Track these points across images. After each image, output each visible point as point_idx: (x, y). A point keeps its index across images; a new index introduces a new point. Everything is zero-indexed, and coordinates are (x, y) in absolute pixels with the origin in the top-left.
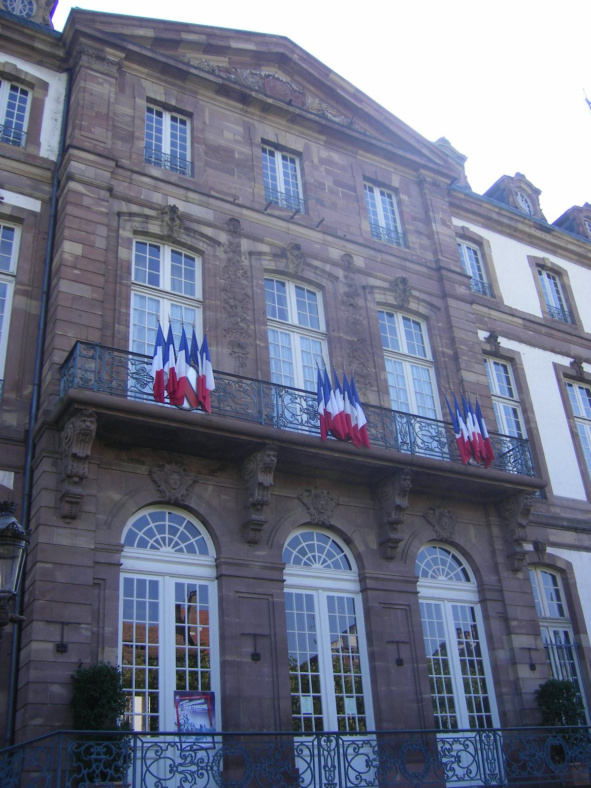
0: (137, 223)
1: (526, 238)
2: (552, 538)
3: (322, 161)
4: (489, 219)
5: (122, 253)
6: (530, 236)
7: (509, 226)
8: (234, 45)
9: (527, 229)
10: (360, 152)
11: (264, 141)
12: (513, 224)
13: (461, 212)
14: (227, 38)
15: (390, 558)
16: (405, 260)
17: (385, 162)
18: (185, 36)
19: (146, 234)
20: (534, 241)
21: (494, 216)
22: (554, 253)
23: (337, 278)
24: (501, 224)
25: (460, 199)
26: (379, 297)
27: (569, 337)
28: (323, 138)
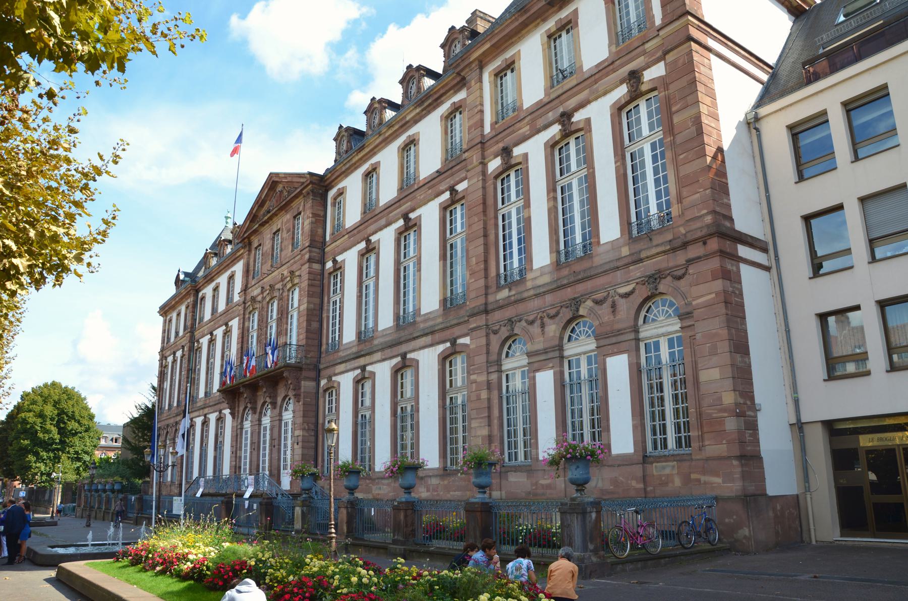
4: (344, 172)
6: (361, 159)
9: (357, 158)
22: (375, 154)
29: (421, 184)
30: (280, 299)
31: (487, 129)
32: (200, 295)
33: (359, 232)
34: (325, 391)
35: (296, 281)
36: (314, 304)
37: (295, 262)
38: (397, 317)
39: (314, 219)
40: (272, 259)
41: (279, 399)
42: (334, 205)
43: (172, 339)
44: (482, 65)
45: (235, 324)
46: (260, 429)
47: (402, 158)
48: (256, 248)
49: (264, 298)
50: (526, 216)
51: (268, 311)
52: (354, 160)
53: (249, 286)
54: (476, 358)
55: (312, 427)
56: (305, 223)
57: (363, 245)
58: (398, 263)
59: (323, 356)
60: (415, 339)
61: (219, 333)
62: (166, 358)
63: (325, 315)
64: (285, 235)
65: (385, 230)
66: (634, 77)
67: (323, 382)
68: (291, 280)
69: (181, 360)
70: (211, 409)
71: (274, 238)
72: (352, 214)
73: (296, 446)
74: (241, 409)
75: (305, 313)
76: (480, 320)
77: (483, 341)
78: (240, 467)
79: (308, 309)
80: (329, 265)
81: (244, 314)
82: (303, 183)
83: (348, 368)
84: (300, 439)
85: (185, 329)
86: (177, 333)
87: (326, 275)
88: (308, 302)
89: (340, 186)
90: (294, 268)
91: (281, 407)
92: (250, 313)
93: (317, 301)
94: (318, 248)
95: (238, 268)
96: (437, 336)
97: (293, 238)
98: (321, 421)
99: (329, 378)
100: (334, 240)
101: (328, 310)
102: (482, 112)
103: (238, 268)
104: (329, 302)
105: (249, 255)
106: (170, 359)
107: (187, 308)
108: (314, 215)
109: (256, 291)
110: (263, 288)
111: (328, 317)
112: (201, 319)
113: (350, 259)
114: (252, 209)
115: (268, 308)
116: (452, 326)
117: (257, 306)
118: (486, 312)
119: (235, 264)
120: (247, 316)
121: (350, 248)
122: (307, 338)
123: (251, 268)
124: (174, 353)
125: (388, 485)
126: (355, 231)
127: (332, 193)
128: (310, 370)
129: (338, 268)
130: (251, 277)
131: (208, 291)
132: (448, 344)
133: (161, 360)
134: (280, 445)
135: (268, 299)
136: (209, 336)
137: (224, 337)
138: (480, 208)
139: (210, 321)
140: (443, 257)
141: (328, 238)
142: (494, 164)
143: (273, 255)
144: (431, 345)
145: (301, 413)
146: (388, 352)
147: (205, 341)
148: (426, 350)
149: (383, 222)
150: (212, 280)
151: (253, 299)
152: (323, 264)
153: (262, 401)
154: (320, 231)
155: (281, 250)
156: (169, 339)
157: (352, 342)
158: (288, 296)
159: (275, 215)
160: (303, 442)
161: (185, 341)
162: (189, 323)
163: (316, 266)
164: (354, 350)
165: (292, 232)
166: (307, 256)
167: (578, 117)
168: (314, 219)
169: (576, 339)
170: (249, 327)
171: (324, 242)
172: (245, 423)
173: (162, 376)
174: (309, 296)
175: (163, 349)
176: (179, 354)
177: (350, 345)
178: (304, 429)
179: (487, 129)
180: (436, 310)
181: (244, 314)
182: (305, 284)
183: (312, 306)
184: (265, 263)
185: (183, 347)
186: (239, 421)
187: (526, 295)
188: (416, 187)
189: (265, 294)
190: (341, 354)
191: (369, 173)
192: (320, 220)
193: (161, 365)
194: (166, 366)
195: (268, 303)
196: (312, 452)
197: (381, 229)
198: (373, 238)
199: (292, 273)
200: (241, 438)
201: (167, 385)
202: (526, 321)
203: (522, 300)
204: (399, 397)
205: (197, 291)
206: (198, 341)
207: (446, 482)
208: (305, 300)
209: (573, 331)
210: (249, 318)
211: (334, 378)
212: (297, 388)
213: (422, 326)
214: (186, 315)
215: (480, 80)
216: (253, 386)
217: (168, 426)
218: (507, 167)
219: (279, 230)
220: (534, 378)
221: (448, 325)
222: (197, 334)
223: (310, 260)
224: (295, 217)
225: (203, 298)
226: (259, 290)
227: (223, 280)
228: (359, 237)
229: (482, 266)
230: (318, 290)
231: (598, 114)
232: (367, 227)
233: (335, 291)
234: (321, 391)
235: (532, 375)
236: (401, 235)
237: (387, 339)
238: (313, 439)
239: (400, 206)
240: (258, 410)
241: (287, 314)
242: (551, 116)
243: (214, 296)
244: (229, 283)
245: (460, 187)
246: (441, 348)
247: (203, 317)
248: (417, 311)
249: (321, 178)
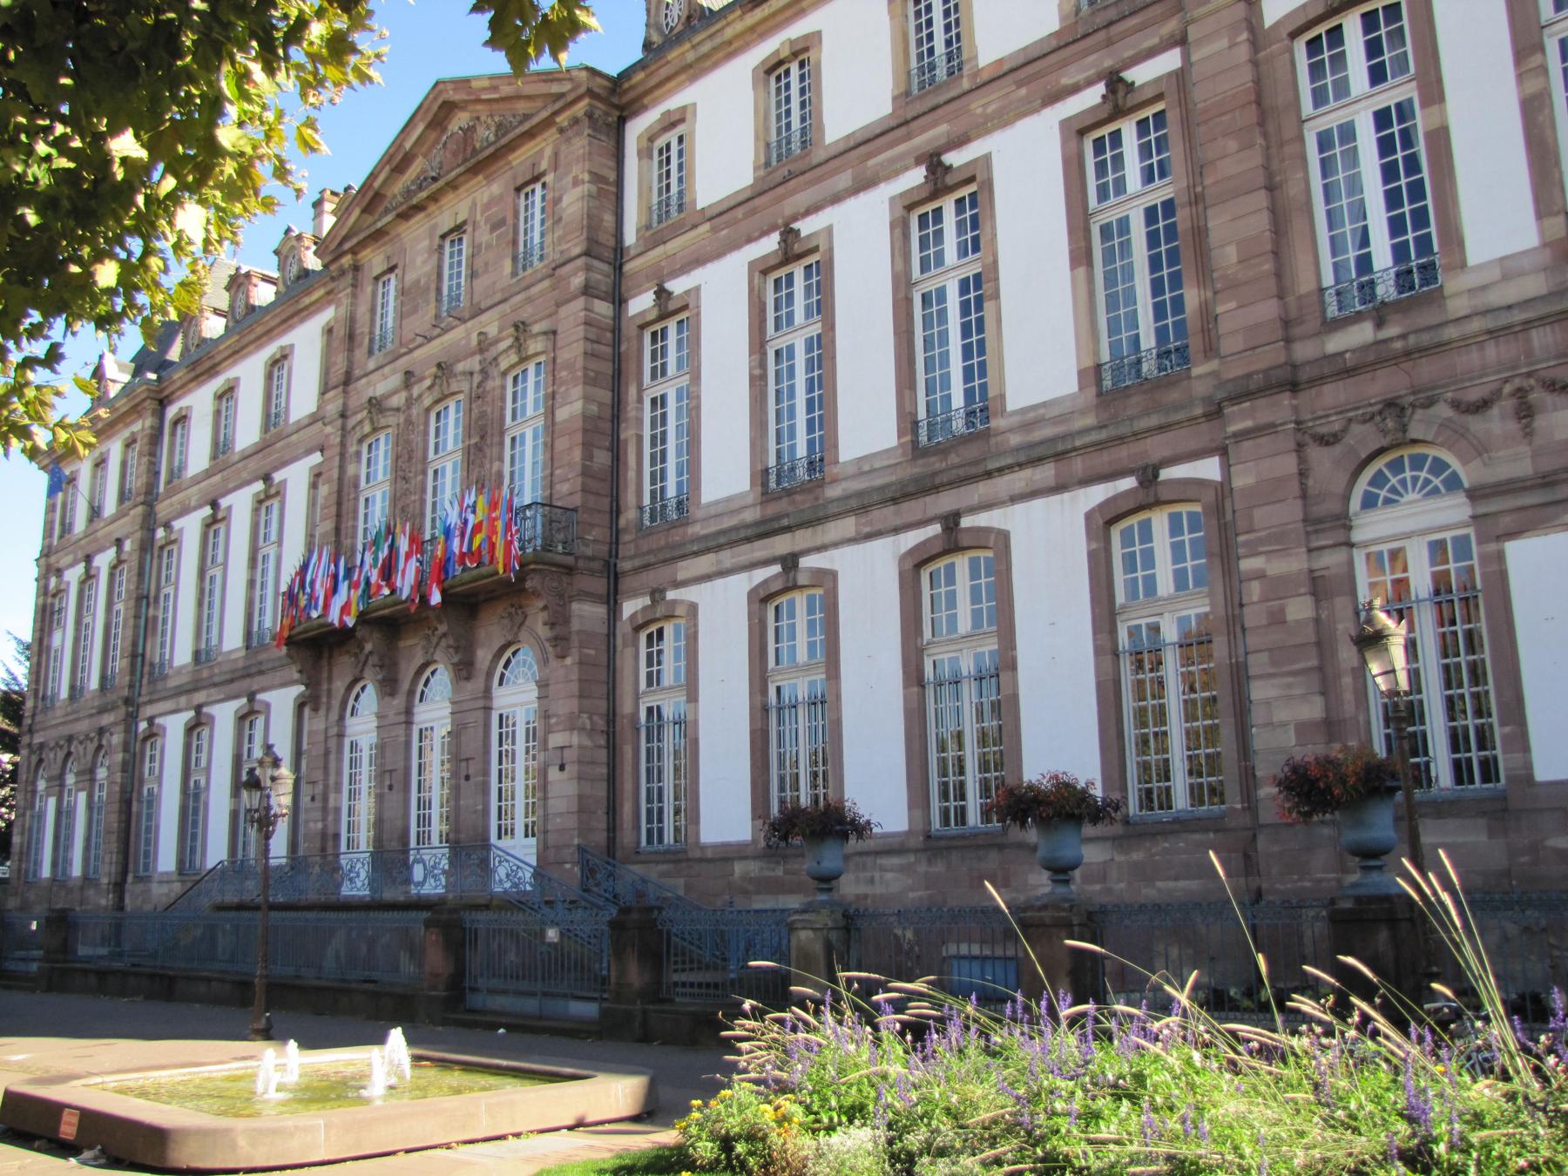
0: (358, 435)
1: (748, 38)
2: (681, 576)
3: (487, 207)
4: (690, 66)
5: (351, 470)
6: (752, 29)
7: (715, 49)
8: (408, 145)
9: (739, 27)
10: (510, 158)
11: (443, 237)
12: (718, 40)
13: (657, 93)
14: (401, 146)
15: (468, 679)
16: (528, 288)
17: (532, 143)
18: (377, 184)
19: (366, 436)
20: (759, 30)
21: (691, 57)
23: (471, 374)
24: (706, 56)
25: (643, 81)
26: (504, 365)
27: (781, 190)
28: (480, 177)
29: (985, 77)
32: (172, 412)
33: (753, 212)
34: (638, 629)
35: (534, 346)
36: (600, 404)
37: (529, 300)
38: (908, 423)
39: (594, 189)
40: (439, 300)
41: (483, 656)
43: (80, 524)
45: (296, 477)
46: (409, 736)
48: (377, 278)
49: (410, 402)
50: (1435, 123)
51: (426, 433)
52: (729, 33)
53: (357, 372)
54: (1258, 513)
55: (601, 723)
57: (770, 244)
59: (626, 538)
60: (989, 475)
61: (240, 503)
62: (59, 572)
63: (627, 433)
64: (484, 236)
65: (851, 204)
67: (631, 607)
68: (518, 345)
69: (112, 576)
70: (215, 693)
71: (441, 247)
73: (554, 774)
74: (339, 686)
75: (579, 424)
76: (1281, 408)
77: (1289, 464)
78: (337, 836)
79: (586, 417)
80: (641, 303)
81: (343, 445)
82: (561, 96)
83: (728, 564)
84: (569, 755)
85: (123, 496)
86: (95, 512)
87: (629, 330)
88: (587, 398)
89: (673, 103)
90: (525, 314)
91: (489, 675)
92: (360, 441)
93: (605, 396)
94: (608, 260)
95: (306, 342)
96: (1078, 465)
97: (515, 242)
98: (626, 707)
99: (657, 594)
100: (653, 237)
101: (640, 421)
103: (306, 342)
104: (640, 400)
105: (354, 296)
106: (74, 575)
107: (129, 445)
108: (597, 178)
109: (384, 384)
110: (408, 374)
111: (640, 438)
112: (174, 474)
113: (721, 290)
114: (373, 176)
115: (427, 424)
116: (1137, 435)
117: (391, 420)
118: (1294, 387)
119: (292, 327)
120: (352, 449)
121: (718, 254)
122: (584, 490)
123: (362, 328)
124: (88, 559)
125: (902, 869)
126: (739, 213)
128: (592, 572)
130: (360, 354)
131: (199, 402)
132: (1128, 483)
133: (43, 579)
134: (486, 773)
135: (427, 401)
136: (207, 511)
137: (256, 511)
138: (1251, 114)
139: (208, 474)
140: (1081, 256)
141: (630, 238)
143: (439, 290)
144: (1059, 488)
145: (574, 687)
146: (887, 515)
147: (190, 527)
148: (1038, 504)
149: (844, 180)
150: (212, 372)
151: (376, 406)
152: (619, 300)
153: (419, 660)
154: (609, 219)
155: (473, 275)
156: (66, 528)
157: (742, 495)
158: (503, 388)
159: (453, 186)
160: (580, 762)
161: (129, 526)
162: (137, 482)
164: (750, 516)
165: (506, 225)
166: (578, 281)
168: (594, 189)
169: (1388, 501)
170: (357, 478)
171: (619, 250)
172: (349, 721)
173: (46, 617)
175: (47, 552)
176: (104, 561)
177: (728, 506)
178: (582, 729)
180: (1072, 397)
181: (343, 445)
183: (594, 408)
184: (415, 310)
185: (119, 543)
186: (334, 716)
187: (1451, 333)
188: (966, 84)
189: (416, 391)
190: (697, 529)
191: (780, 63)
193: (43, 591)
195: (428, 410)
196: (601, 791)
197: (836, 199)
199: (521, 328)
200: (340, 760)
201: (62, 639)
202: (1456, 405)
203: (1439, 347)
204: (927, 634)
205: (163, 403)
206: (167, 526)
207: (1137, 856)
208: (577, 391)
209: (1378, 480)
210: (358, 454)
211: (671, 595)
212: (559, 620)
213: (1015, 440)
214: (124, 464)
216: (389, 625)
217: (70, 739)
219: (459, 228)
220: (1500, 557)
221: (1124, 430)
222: (163, 509)
223: (588, 291)
224: (518, 190)
225: (182, 419)
226: (395, 380)
227: (249, 372)
229: (1268, 267)
230: (607, 368)
232: (783, 198)
233: (659, 372)
234: (623, 628)
235: (1492, 547)
236: (915, 214)
237: (879, 481)
238: (602, 755)
239: (909, 137)
240: (405, 686)
241: (502, 433)
243: (218, 413)
244: (269, 377)
246: (1097, 494)
247: (183, 467)
248: (982, 405)
249: (617, 83)
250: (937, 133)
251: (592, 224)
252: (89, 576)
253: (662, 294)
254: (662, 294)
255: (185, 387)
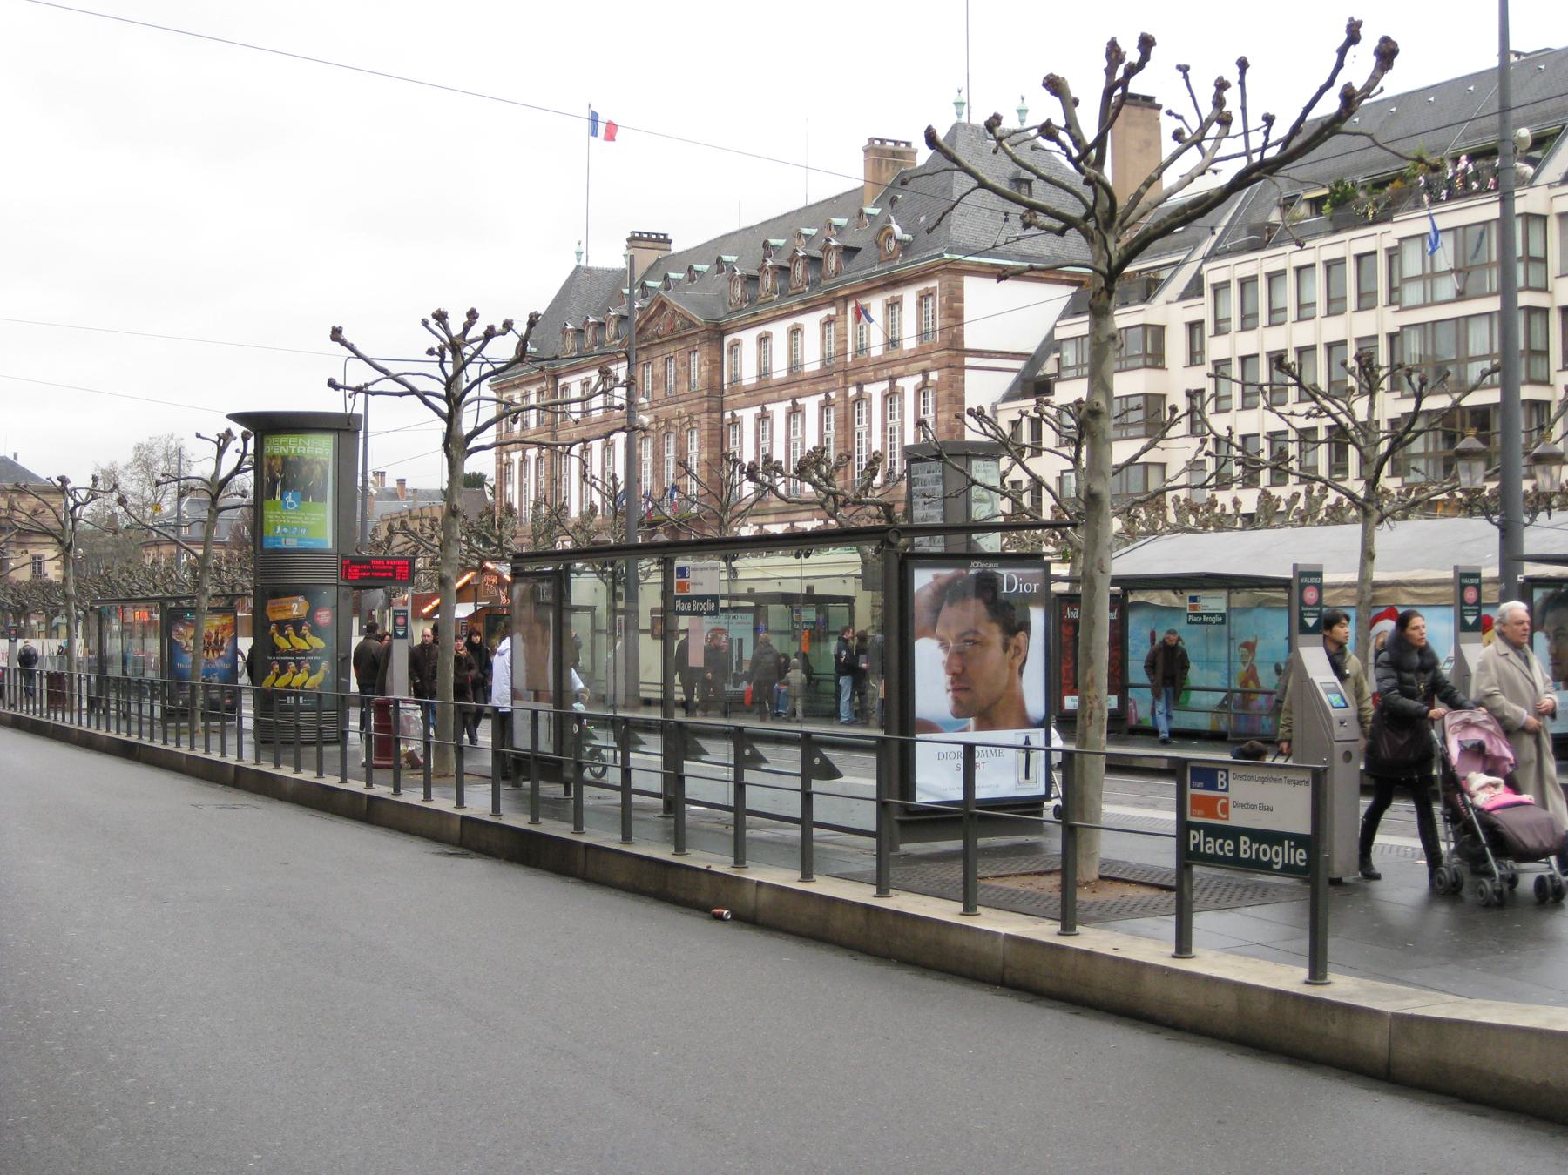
30: (678, 438)
31: (849, 359)
32: (561, 382)
42: (730, 352)
44: (846, 299)
47: (791, 340)
56: (699, 367)
58: (788, 440)
62: (508, 453)
66: (925, 373)
72: (749, 376)
80: (728, 415)
93: (717, 450)
102: (846, 341)
106: (516, 456)
127: (728, 339)
129: (736, 422)
142: (853, 391)
146: (781, 517)
149: (775, 395)
154: (717, 378)
163: (716, 415)
165: (687, 365)
167: (899, 383)
174: (709, 446)
179: (849, 359)
182: (705, 433)
192: (717, 366)
194: (509, 464)
198: (769, 407)
199: (690, 415)
205: (556, 377)
215: (845, 313)
218: (860, 398)
223: (709, 410)
228: (755, 399)
231: (909, 384)
242: (886, 373)
245: (833, 395)
250: (794, 391)
251: (711, 379)
252: (524, 461)
253: (733, 415)
254: (733, 415)
255: (566, 374)
